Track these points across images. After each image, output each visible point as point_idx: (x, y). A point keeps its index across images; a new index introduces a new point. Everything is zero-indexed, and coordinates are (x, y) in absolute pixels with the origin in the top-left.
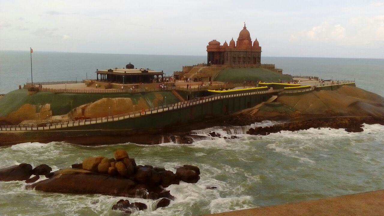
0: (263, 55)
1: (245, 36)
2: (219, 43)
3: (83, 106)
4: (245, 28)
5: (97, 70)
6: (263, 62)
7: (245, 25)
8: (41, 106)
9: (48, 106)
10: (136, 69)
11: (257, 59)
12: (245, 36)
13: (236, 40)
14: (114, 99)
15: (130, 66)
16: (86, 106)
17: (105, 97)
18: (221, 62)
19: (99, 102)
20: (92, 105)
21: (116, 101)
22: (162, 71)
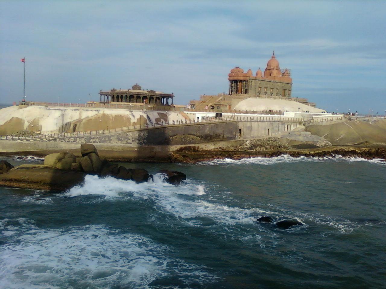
0: (293, 87)
5: (101, 91)
6: (293, 93)
7: (274, 54)
10: (144, 90)
11: (287, 91)
13: (263, 71)
15: (136, 87)
18: (244, 92)
21: (112, 117)
22: (173, 93)
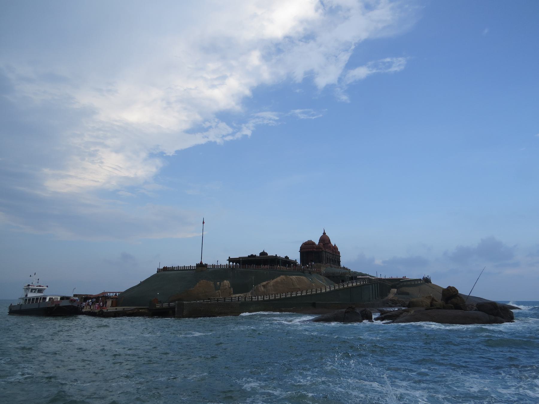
0: (342, 259)
1: (325, 240)
2: (313, 243)
3: (264, 283)
4: (324, 233)
8: (218, 283)
9: (226, 283)
12: (325, 240)
14: (291, 277)
16: (267, 284)
17: (283, 275)
19: (278, 279)
20: (272, 282)
